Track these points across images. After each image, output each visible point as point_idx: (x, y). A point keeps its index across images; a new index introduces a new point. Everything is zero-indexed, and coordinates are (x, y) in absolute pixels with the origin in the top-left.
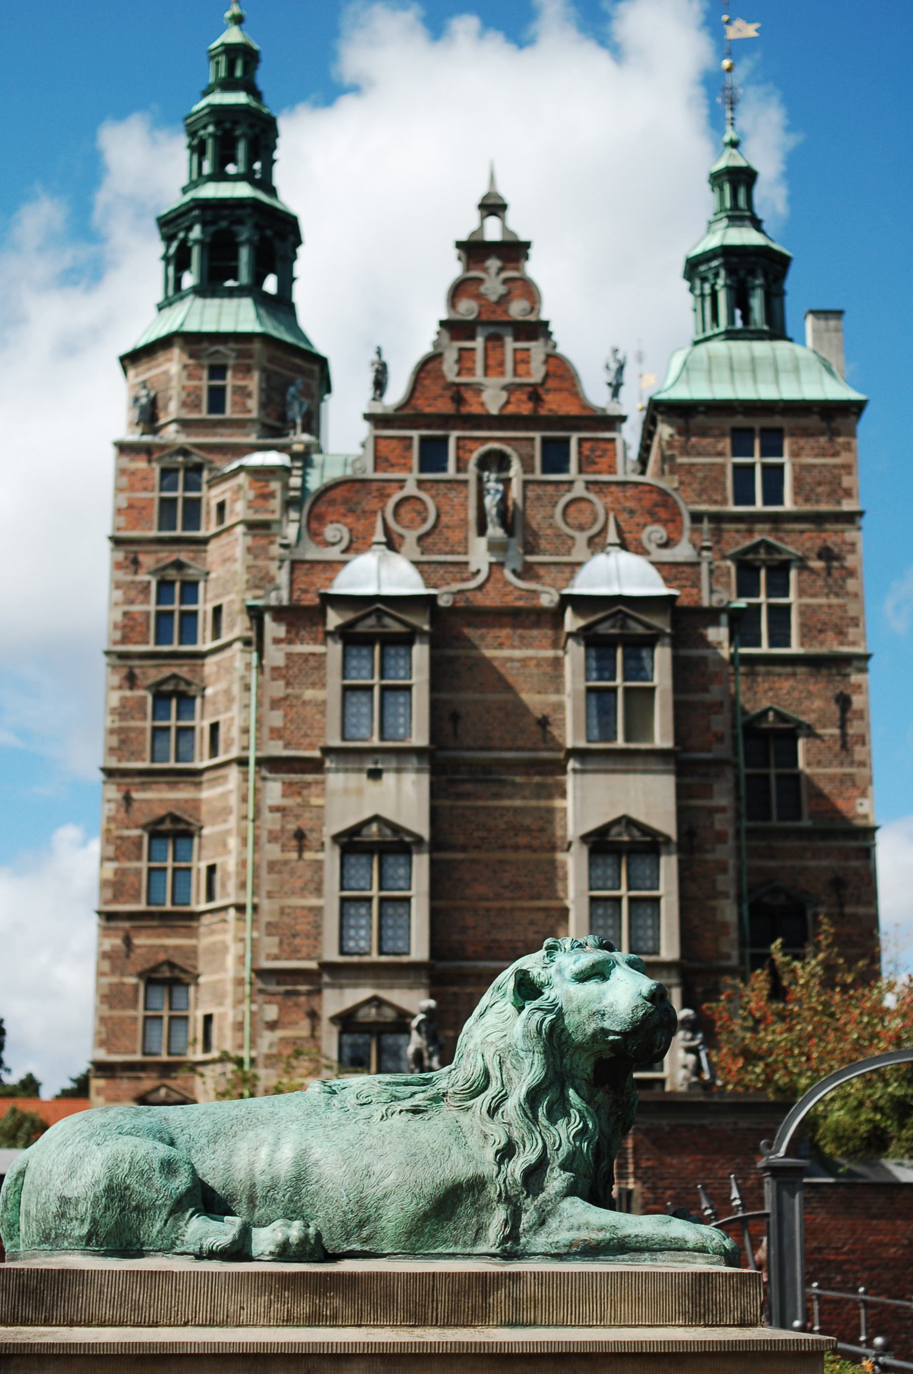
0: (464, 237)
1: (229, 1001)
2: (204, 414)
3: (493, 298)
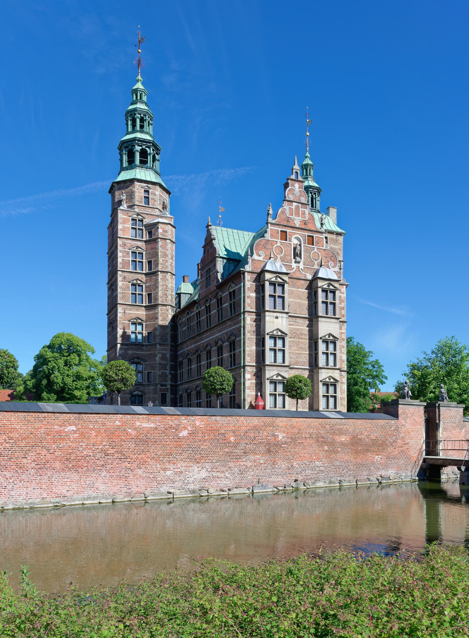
1: (157, 369)
2: (143, 204)
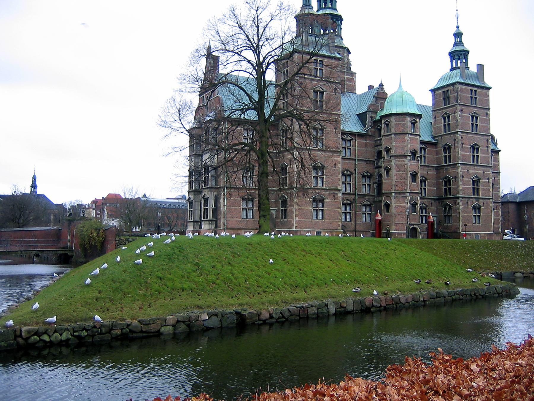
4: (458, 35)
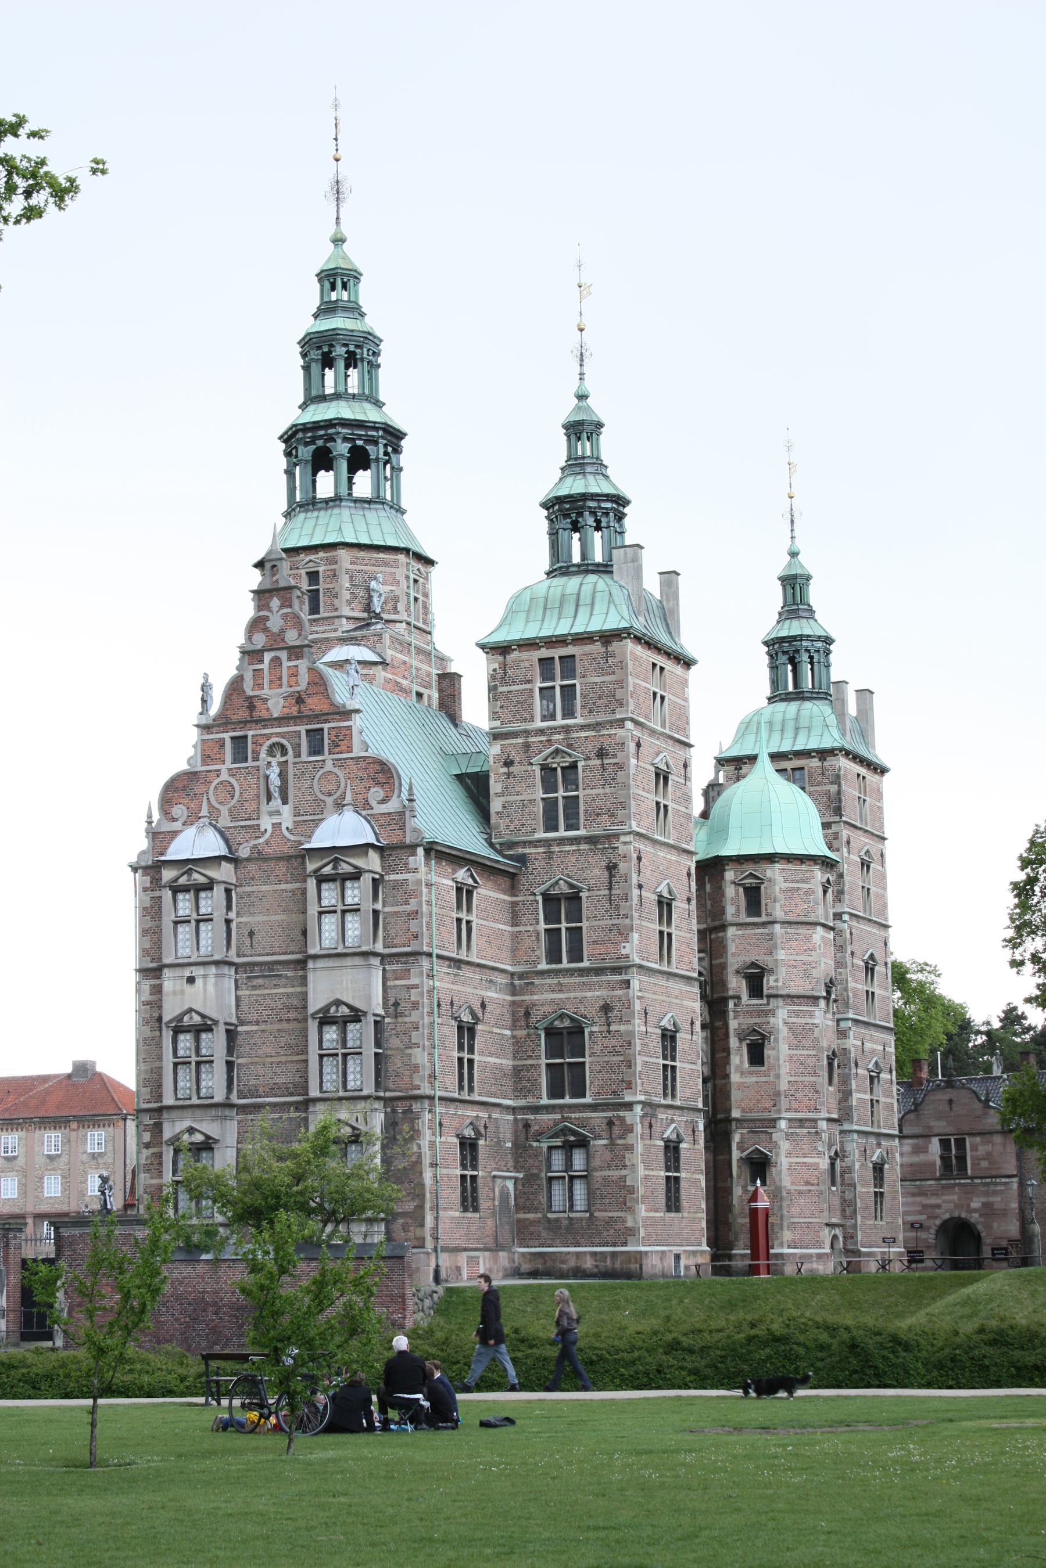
0: (255, 588)
3: (275, 630)
4: (794, 585)
